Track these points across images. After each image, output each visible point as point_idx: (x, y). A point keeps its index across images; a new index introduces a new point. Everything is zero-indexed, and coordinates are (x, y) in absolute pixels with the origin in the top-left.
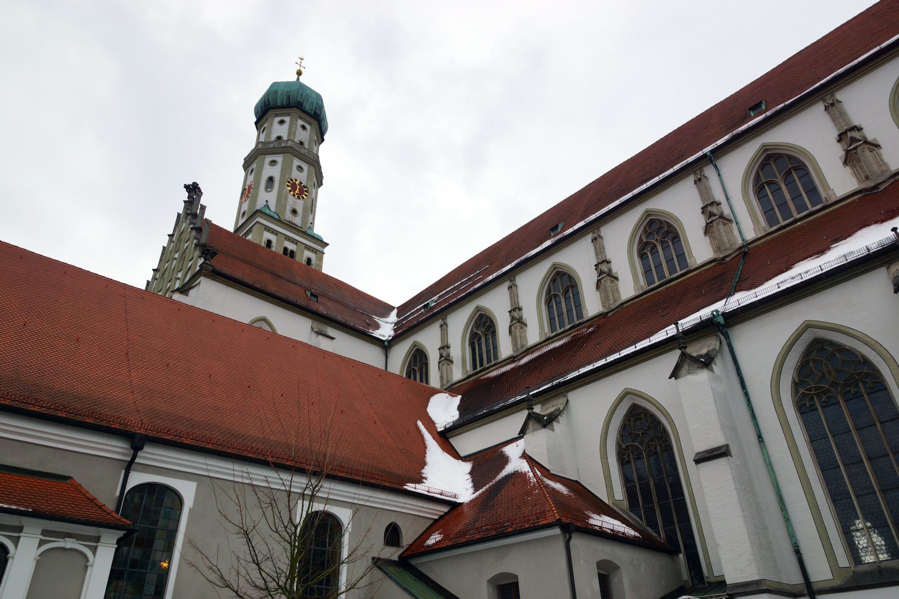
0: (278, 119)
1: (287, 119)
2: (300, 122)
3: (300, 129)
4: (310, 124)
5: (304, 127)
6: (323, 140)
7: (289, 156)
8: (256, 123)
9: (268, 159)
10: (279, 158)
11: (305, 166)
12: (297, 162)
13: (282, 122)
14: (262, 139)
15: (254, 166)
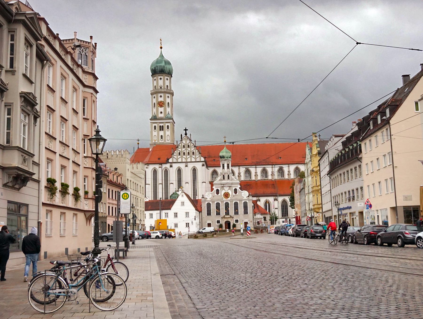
0: (159, 77)
1: (162, 77)
2: (166, 78)
3: (166, 80)
4: (169, 77)
5: (167, 79)
6: (172, 77)
7: (165, 94)
8: (152, 75)
9: (159, 95)
10: (162, 95)
11: (169, 95)
12: (167, 95)
13: (161, 79)
14: (155, 84)
15: (155, 95)
